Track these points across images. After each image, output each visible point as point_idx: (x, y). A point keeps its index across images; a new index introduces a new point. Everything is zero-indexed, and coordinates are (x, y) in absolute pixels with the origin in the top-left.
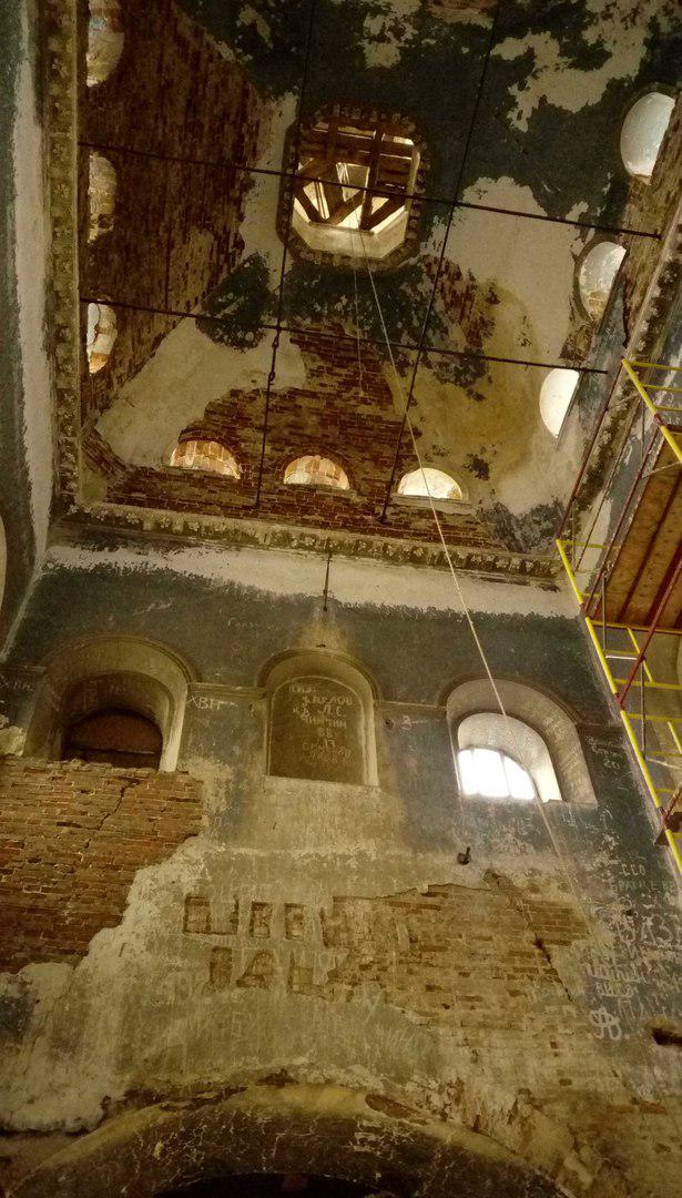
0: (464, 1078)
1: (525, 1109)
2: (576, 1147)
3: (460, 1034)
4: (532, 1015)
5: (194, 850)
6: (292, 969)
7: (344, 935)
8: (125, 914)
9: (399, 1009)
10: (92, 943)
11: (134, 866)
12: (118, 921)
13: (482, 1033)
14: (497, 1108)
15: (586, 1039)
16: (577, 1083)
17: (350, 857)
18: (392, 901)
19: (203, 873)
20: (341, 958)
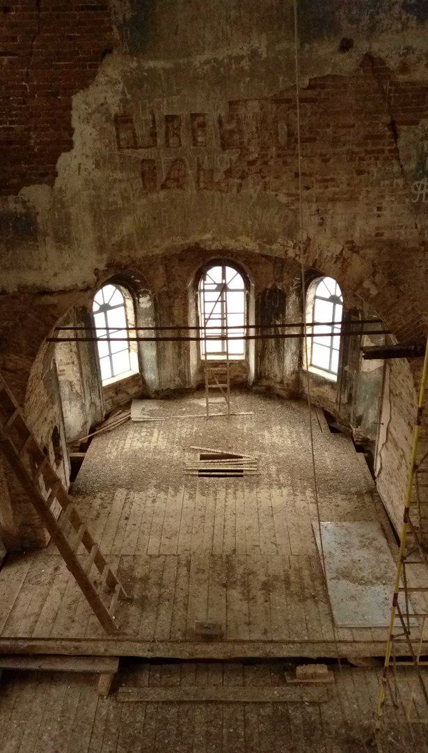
0: (311, 236)
1: (347, 254)
2: (374, 275)
3: (314, 207)
4: (369, 189)
5: (113, 69)
6: (199, 170)
7: (236, 137)
8: (74, 138)
9: (274, 193)
10: (58, 166)
11: (70, 91)
12: (69, 145)
13: (330, 206)
14: (330, 254)
15: (404, 203)
16: (387, 235)
17: (242, 57)
18: (277, 101)
19: (123, 92)
20: (234, 158)
